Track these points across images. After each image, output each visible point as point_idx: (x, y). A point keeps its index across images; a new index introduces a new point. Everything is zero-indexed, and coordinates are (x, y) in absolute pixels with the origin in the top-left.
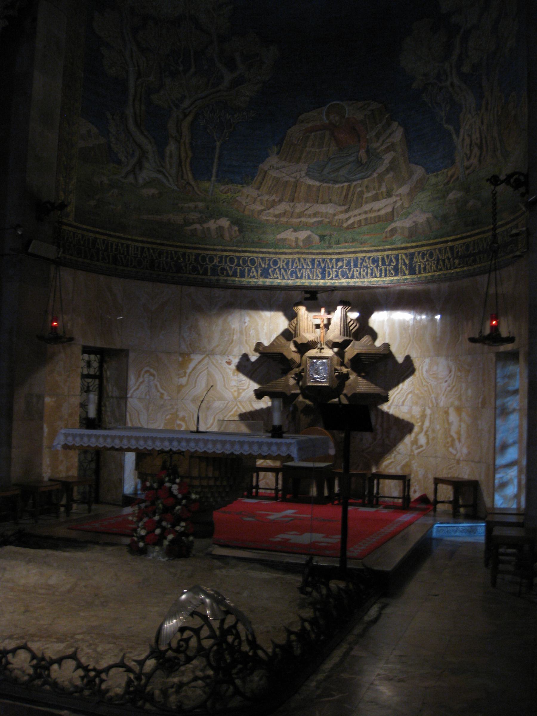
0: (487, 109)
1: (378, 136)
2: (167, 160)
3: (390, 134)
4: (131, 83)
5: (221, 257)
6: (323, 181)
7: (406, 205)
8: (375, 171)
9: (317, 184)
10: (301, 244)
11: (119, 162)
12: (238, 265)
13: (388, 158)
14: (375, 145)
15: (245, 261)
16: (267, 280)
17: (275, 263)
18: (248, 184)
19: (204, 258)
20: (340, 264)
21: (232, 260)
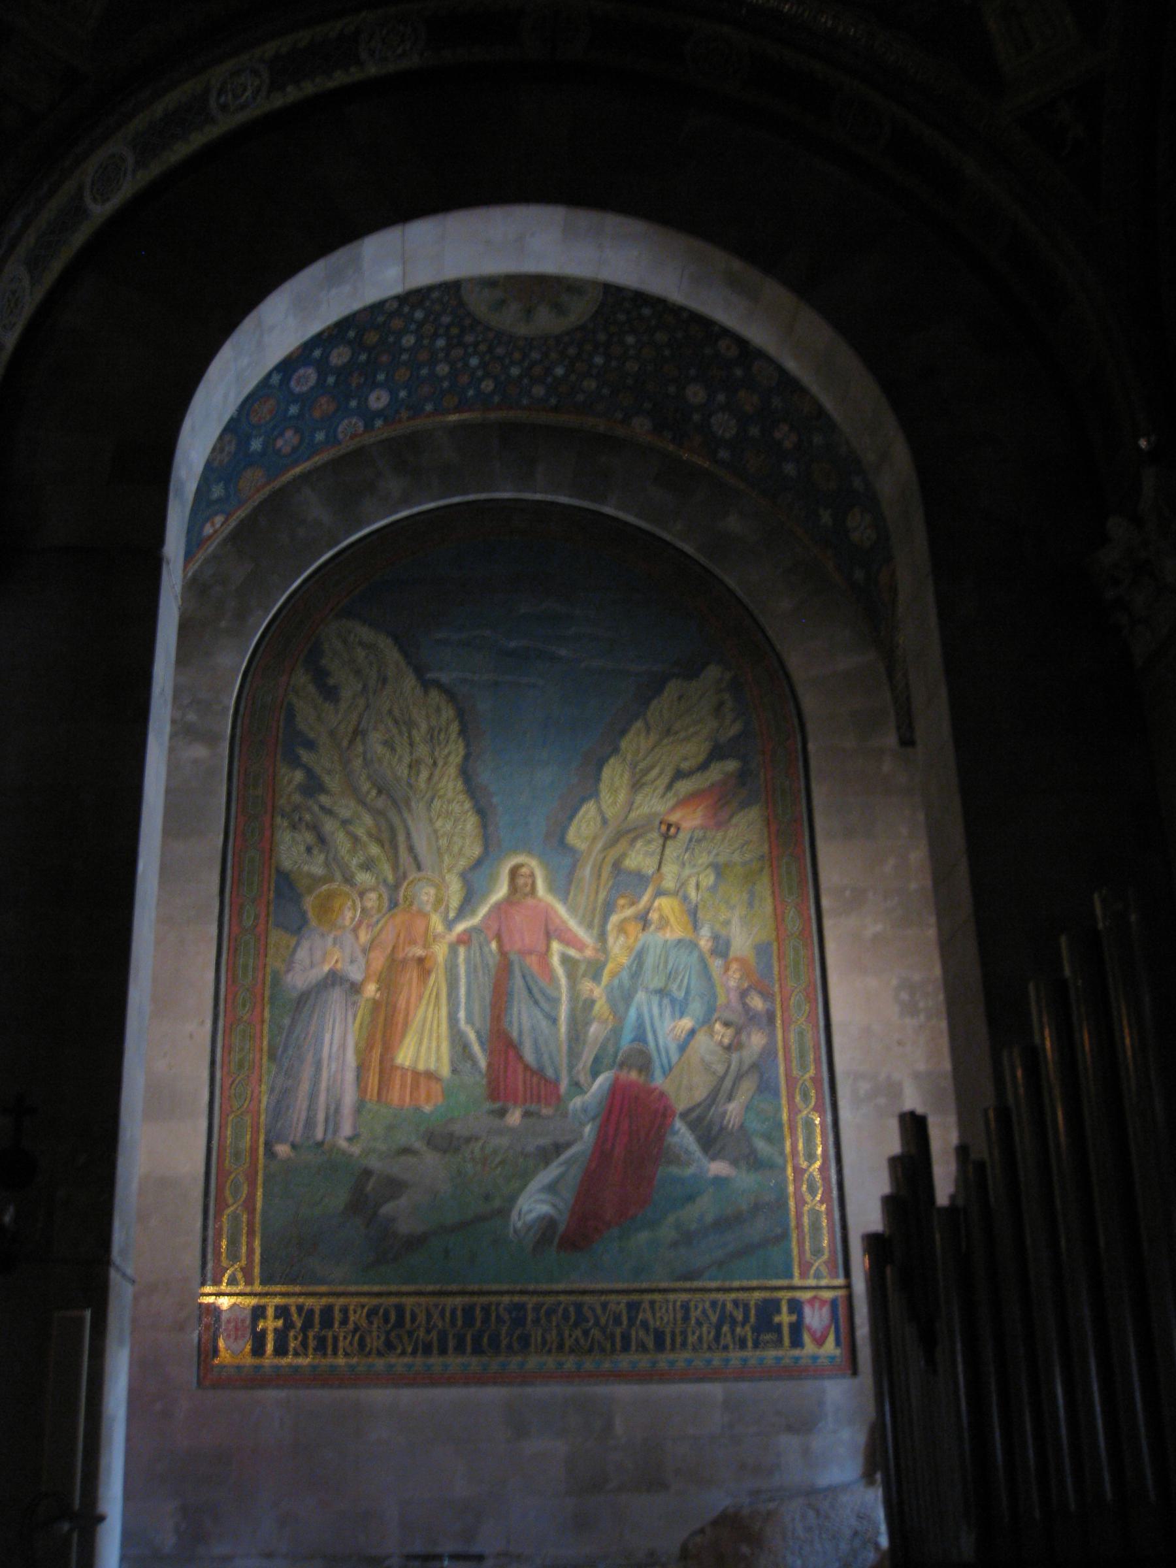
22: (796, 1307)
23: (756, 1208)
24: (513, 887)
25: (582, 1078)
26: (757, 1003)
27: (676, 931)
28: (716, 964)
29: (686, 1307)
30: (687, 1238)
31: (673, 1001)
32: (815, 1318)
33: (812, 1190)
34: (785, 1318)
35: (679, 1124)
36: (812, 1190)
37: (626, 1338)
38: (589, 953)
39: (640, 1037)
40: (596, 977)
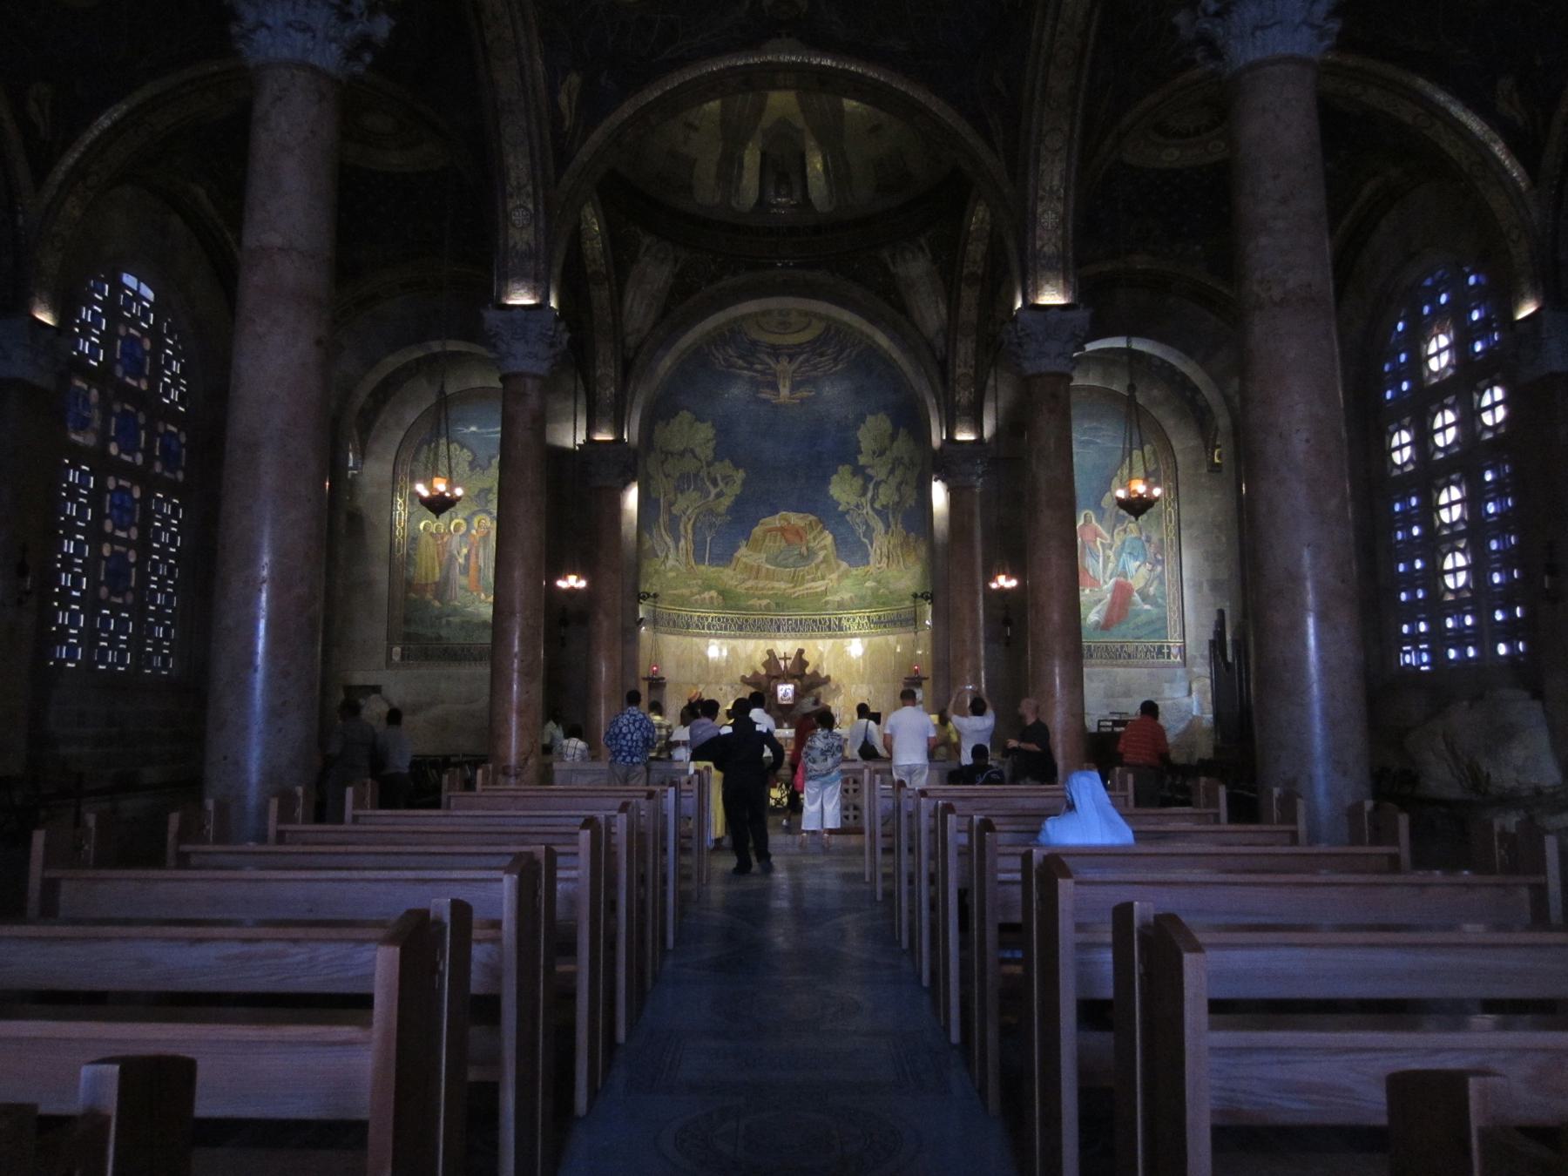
0: (892, 536)
1: (815, 539)
2: (680, 551)
3: (823, 539)
4: (662, 500)
5: (712, 618)
6: (777, 565)
7: (836, 585)
8: (812, 561)
9: (773, 568)
10: (763, 608)
11: (657, 556)
12: (723, 622)
13: (822, 554)
14: (811, 545)
15: (727, 620)
16: (742, 633)
17: (747, 621)
18: (727, 567)
19: (702, 618)
20: (790, 622)
21: (719, 620)
22: (1169, 647)
23: (1159, 619)
24: (1085, 521)
25: (1107, 580)
26: (1160, 557)
27: (1135, 535)
28: (1147, 545)
29: (1137, 647)
30: (1138, 627)
31: (1134, 556)
32: (1174, 651)
33: (1174, 614)
34: (1166, 651)
35: (1136, 594)
36: (1174, 614)
37: (1120, 655)
38: (1109, 541)
39: (1124, 567)
40: (1111, 548)
